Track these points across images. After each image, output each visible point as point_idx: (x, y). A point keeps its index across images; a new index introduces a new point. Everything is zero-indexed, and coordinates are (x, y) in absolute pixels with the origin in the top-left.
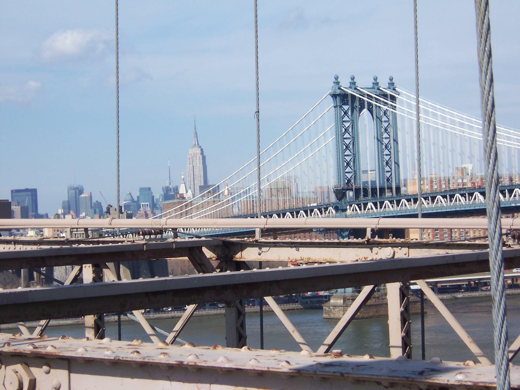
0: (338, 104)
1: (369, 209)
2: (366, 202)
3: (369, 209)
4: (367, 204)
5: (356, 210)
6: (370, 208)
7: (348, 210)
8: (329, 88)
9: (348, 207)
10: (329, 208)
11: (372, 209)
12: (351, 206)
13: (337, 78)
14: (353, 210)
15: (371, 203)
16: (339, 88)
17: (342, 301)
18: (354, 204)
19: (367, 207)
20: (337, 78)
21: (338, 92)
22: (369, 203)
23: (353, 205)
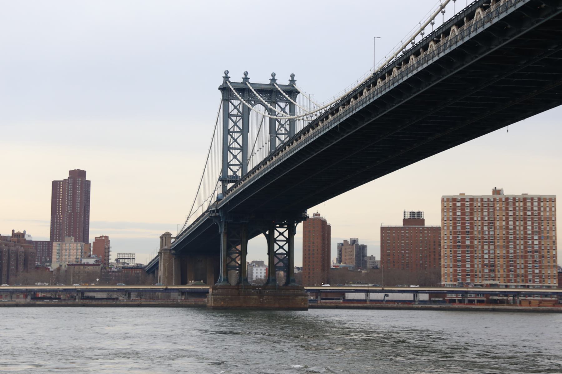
13: (227, 73)
20: (227, 73)
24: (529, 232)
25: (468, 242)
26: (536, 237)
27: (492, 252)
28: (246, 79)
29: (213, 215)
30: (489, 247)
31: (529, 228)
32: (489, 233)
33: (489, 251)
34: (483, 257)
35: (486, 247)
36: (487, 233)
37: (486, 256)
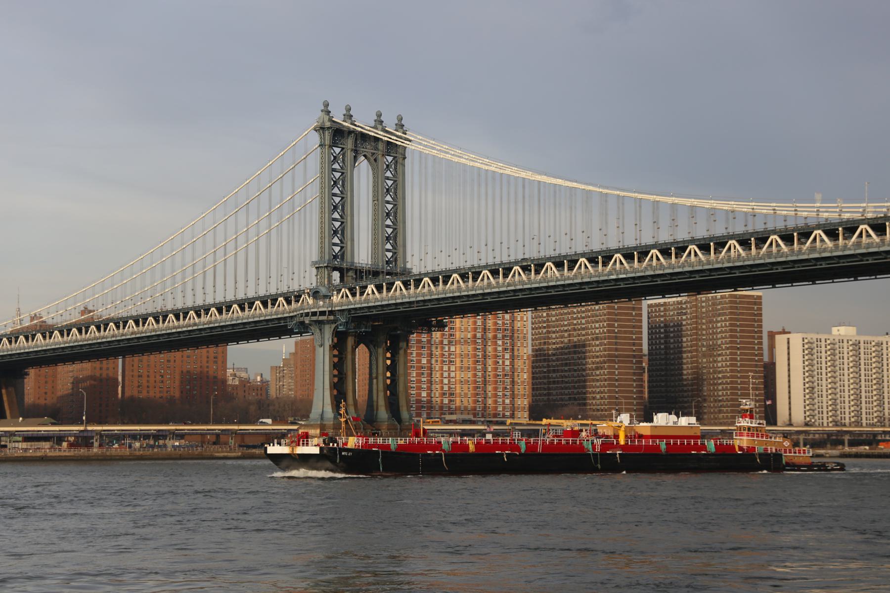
0: (327, 142)
1: (368, 294)
2: (364, 284)
3: (368, 294)
4: (366, 287)
5: (347, 296)
6: (370, 292)
7: (335, 297)
8: (315, 117)
9: (335, 293)
10: (303, 296)
11: (373, 293)
12: (339, 291)
13: (326, 105)
14: (342, 297)
15: (372, 286)
16: (331, 120)
17: (318, 431)
18: (345, 287)
19: (365, 291)
20: (326, 105)
21: (328, 124)
22: (369, 286)
23: (343, 290)
24: (500, 349)
25: (424, 361)
26: (507, 356)
27: (453, 374)
28: (349, 116)
29: (321, 318)
30: (449, 368)
31: (500, 342)
32: (449, 348)
33: (449, 374)
34: (442, 382)
35: (446, 368)
36: (447, 349)
37: (446, 381)
